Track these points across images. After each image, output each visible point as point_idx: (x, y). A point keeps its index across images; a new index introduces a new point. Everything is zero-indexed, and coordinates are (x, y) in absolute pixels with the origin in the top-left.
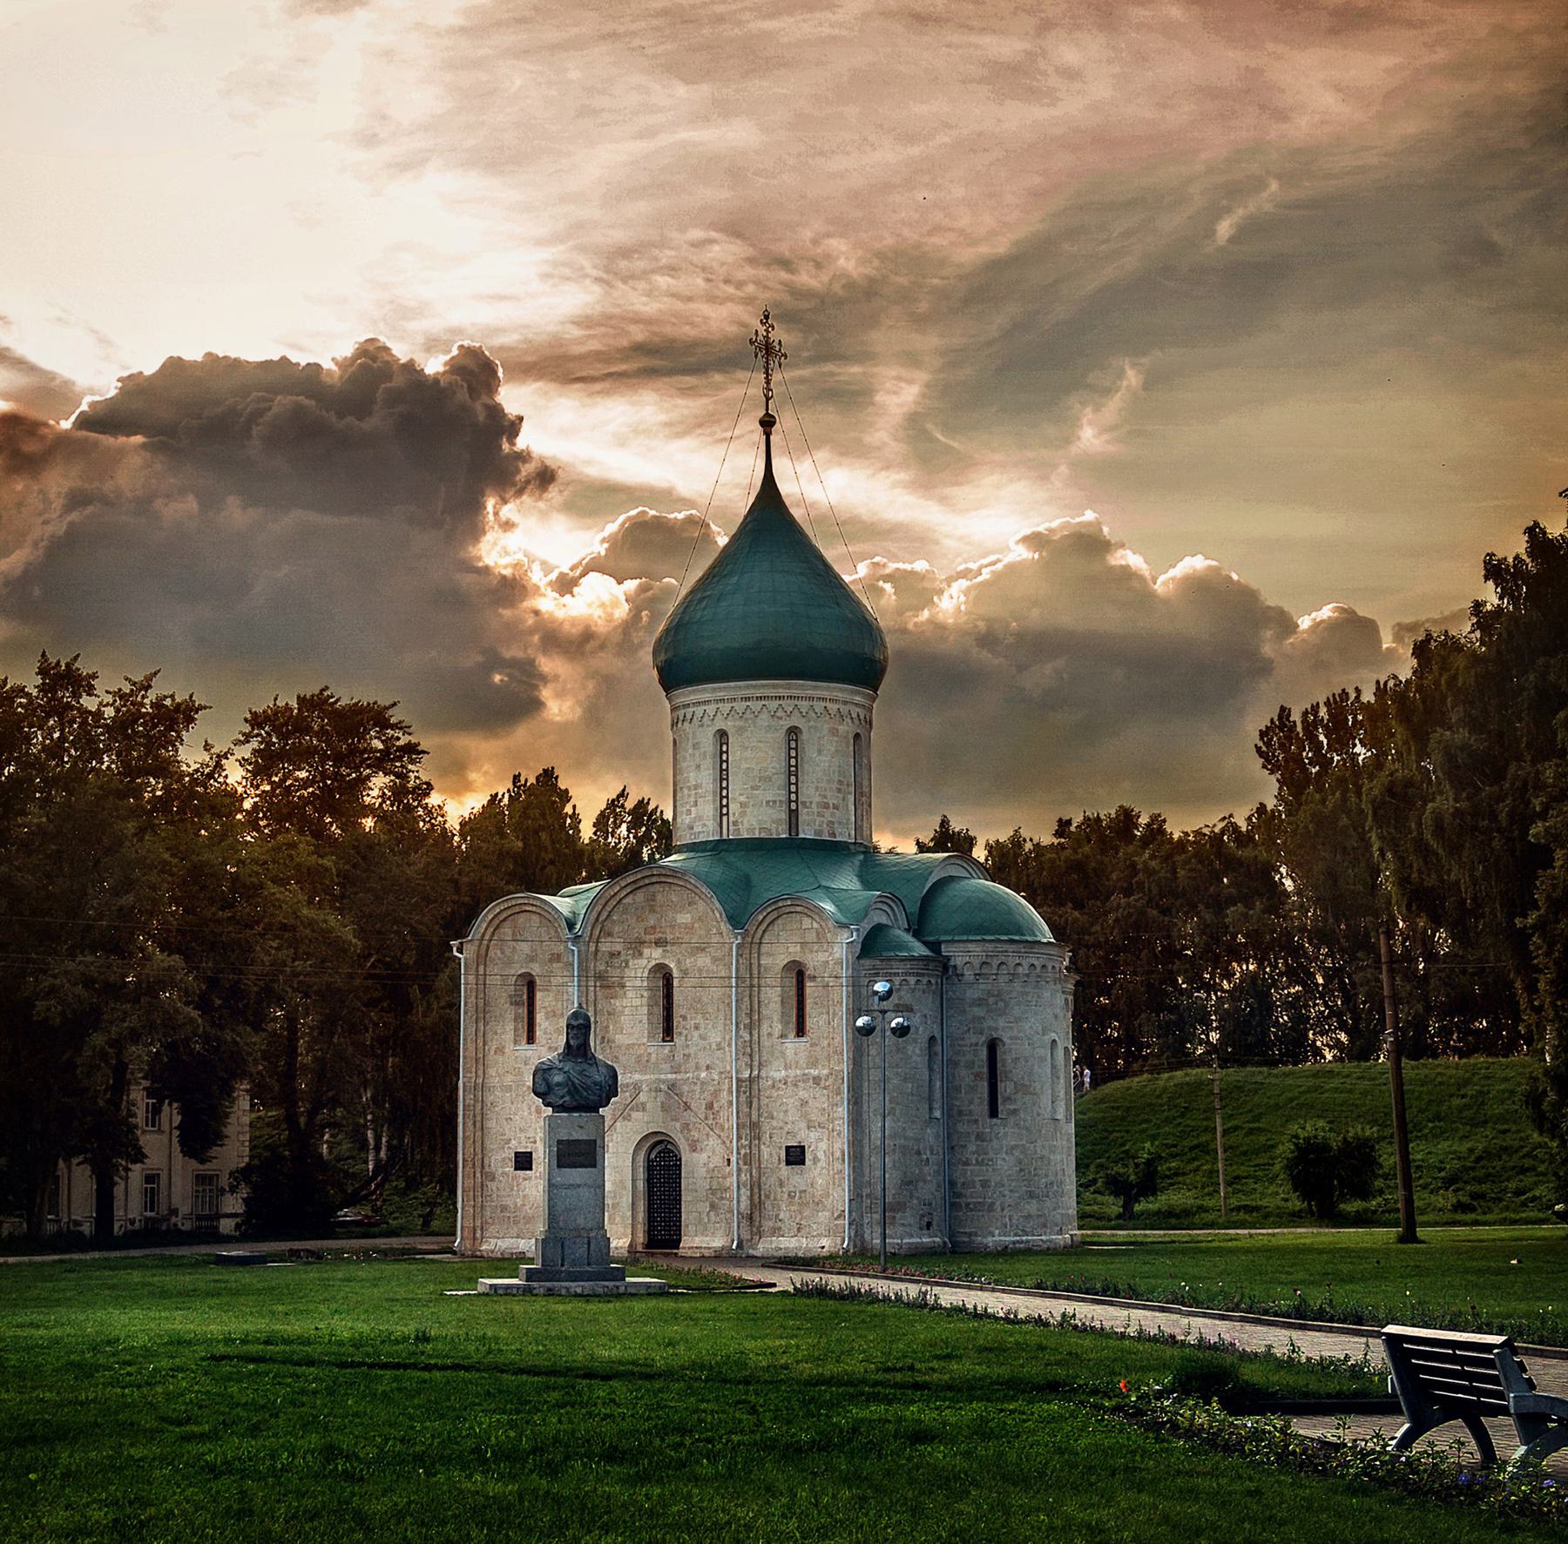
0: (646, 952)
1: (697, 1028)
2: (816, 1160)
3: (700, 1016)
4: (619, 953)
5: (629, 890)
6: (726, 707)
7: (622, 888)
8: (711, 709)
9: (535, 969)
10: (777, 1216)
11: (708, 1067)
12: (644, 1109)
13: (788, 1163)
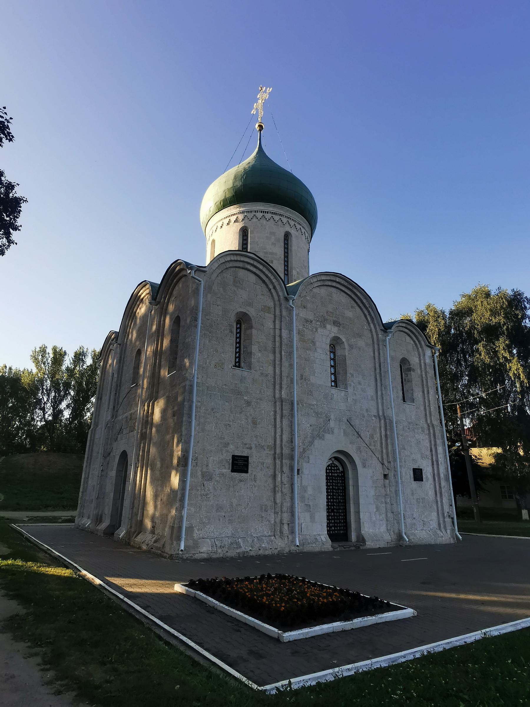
0: (328, 327)
1: (360, 383)
2: (427, 479)
3: (361, 376)
5: (319, 284)
7: (318, 281)
8: (285, 220)
9: (252, 312)
12: (333, 433)
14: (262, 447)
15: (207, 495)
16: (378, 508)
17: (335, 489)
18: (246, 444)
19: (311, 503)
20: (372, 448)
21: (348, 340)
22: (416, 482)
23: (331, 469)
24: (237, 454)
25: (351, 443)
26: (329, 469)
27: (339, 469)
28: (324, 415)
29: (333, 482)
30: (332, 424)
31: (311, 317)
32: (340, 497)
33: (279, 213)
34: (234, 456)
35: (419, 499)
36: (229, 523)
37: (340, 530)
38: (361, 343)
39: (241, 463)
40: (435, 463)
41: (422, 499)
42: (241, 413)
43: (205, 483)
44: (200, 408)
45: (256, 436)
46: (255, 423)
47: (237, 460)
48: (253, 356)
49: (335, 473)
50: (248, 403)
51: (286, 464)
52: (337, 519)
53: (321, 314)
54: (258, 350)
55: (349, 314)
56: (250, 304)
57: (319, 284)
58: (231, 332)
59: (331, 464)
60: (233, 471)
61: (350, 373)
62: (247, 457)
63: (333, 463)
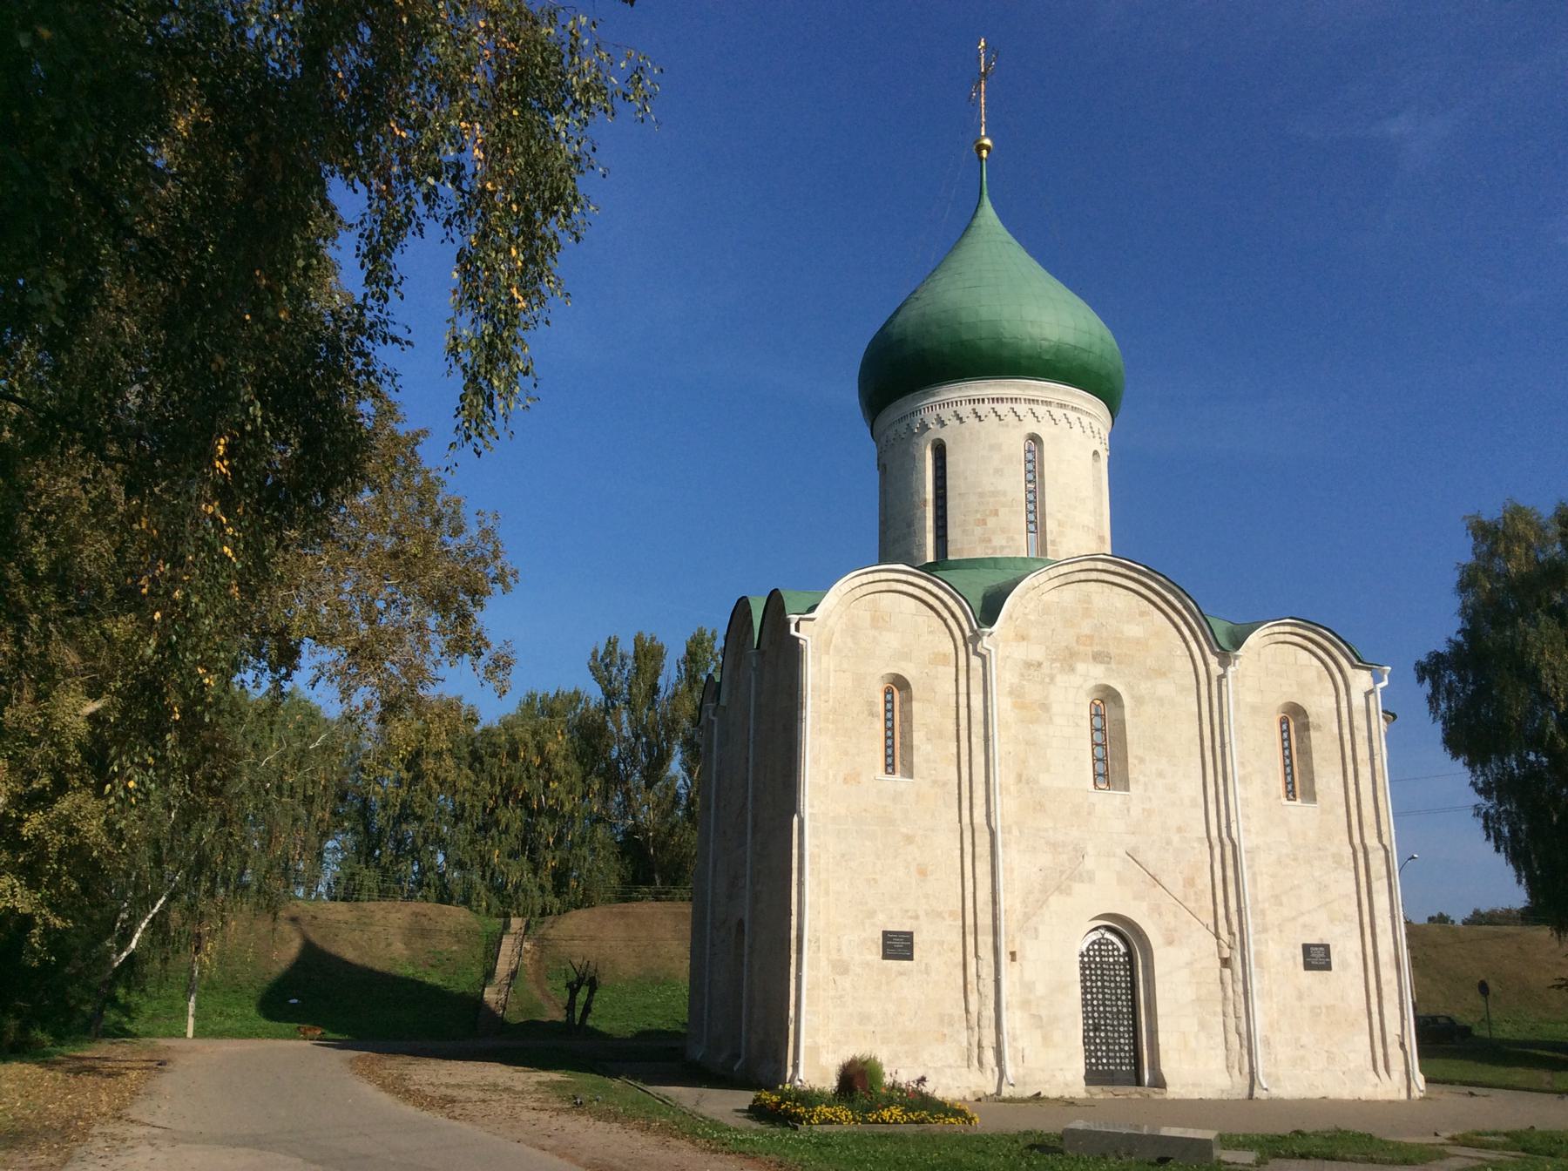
0: (1081, 667)
2: (1345, 965)
4: (1040, 665)
5: (1056, 582)
6: (1041, 410)
8: (1022, 408)
9: (909, 672)
10: (1297, 1040)
11: (1179, 829)
12: (1091, 879)
13: (1308, 966)
14: (939, 915)
15: (841, 997)
16: (1203, 1026)
17: (1109, 988)
18: (907, 911)
19: (1043, 1013)
20: (1191, 905)
21: (1130, 687)
22: (1310, 972)
23: (1100, 950)
24: (890, 928)
25: (1135, 898)
26: (1094, 950)
27: (1118, 950)
28: (1070, 848)
29: (1103, 975)
30: (1089, 863)
31: (1037, 653)
32: (1120, 1003)
33: (1009, 396)
34: (885, 934)
35: (1320, 1008)
36: (883, 1043)
37: (1121, 1064)
38: (1164, 688)
39: (898, 943)
40: (1367, 928)
41: (1327, 1007)
42: (896, 857)
43: (837, 978)
44: (819, 857)
45: (927, 896)
46: (923, 873)
47: (891, 939)
48: (915, 752)
49: (1109, 956)
50: (909, 839)
51: (985, 944)
52: (1115, 1044)
53: (1064, 644)
54: (925, 739)
55: (1134, 630)
56: (906, 656)
57: (1056, 582)
58: (872, 714)
59: (1099, 939)
60: (886, 956)
61: (1136, 757)
62: (911, 934)
63: (1103, 938)
